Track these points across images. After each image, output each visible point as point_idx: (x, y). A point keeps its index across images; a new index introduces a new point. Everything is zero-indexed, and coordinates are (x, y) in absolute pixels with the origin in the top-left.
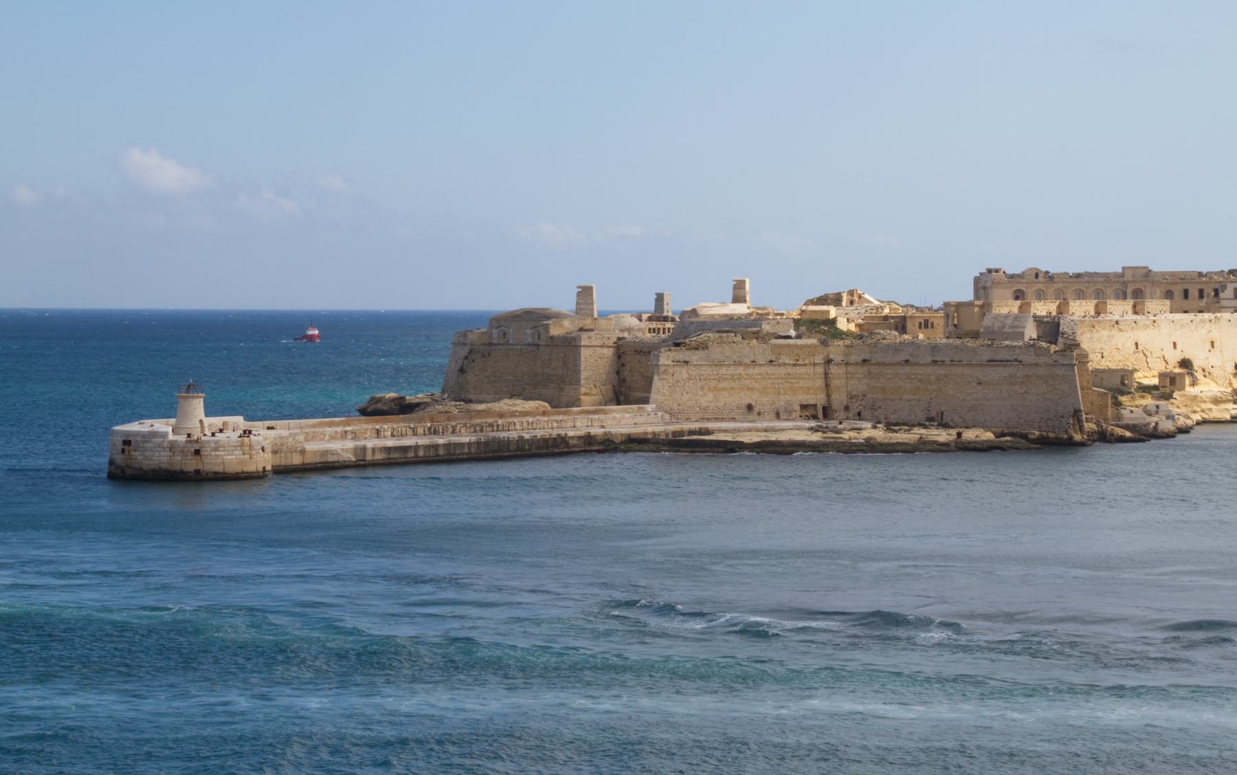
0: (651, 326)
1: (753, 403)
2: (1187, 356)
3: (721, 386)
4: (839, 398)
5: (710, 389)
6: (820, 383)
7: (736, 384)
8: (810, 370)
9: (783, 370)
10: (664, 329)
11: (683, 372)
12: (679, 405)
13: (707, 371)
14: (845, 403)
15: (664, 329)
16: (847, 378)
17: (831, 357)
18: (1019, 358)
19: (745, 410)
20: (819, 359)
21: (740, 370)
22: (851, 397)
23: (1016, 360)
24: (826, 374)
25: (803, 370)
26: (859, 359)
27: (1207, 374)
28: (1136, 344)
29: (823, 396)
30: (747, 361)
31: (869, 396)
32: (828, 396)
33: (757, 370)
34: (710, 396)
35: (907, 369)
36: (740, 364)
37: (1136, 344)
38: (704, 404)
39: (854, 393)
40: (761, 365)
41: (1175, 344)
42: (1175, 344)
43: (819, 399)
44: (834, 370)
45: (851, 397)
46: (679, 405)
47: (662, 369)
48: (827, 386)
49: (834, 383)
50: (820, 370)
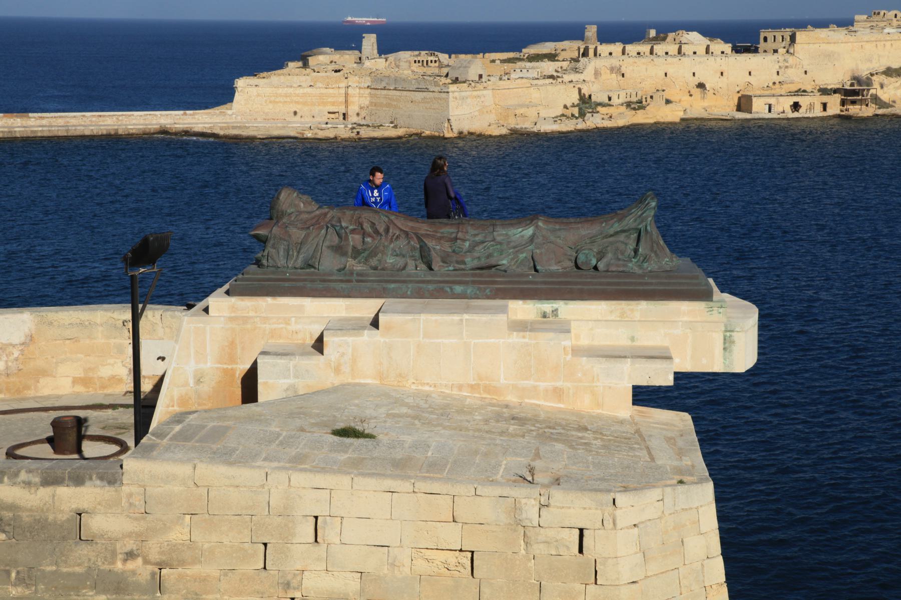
0: (416, 59)
1: (298, 111)
2: (702, 80)
3: (277, 100)
4: (353, 109)
5: (271, 102)
6: (342, 99)
7: (288, 99)
8: (336, 91)
9: (318, 91)
10: (427, 61)
11: (254, 91)
12: (250, 111)
13: (268, 90)
14: (357, 112)
15: (427, 61)
16: (359, 97)
17: (350, 84)
18: (428, 87)
19: (293, 115)
20: (343, 85)
21: (290, 90)
22: (361, 108)
23: (426, 88)
24: (347, 95)
25: (331, 91)
26: (366, 86)
27: (716, 92)
28: (666, 74)
29: (344, 107)
30: (295, 85)
31: (370, 108)
32: (347, 107)
33: (300, 91)
34: (271, 106)
35: (385, 92)
36: (291, 87)
37: (666, 74)
38: (266, 111)
39: (362, 106)
40: (304, 88)
41: (694, 74)
42: (694, 74)
43: (342, 109)
44: (350, 91)
45: (361, 108)
46: (250, 111)
47: (239, 89)
48: (346, 101)
49: (350, 99)
50: (343, 91)
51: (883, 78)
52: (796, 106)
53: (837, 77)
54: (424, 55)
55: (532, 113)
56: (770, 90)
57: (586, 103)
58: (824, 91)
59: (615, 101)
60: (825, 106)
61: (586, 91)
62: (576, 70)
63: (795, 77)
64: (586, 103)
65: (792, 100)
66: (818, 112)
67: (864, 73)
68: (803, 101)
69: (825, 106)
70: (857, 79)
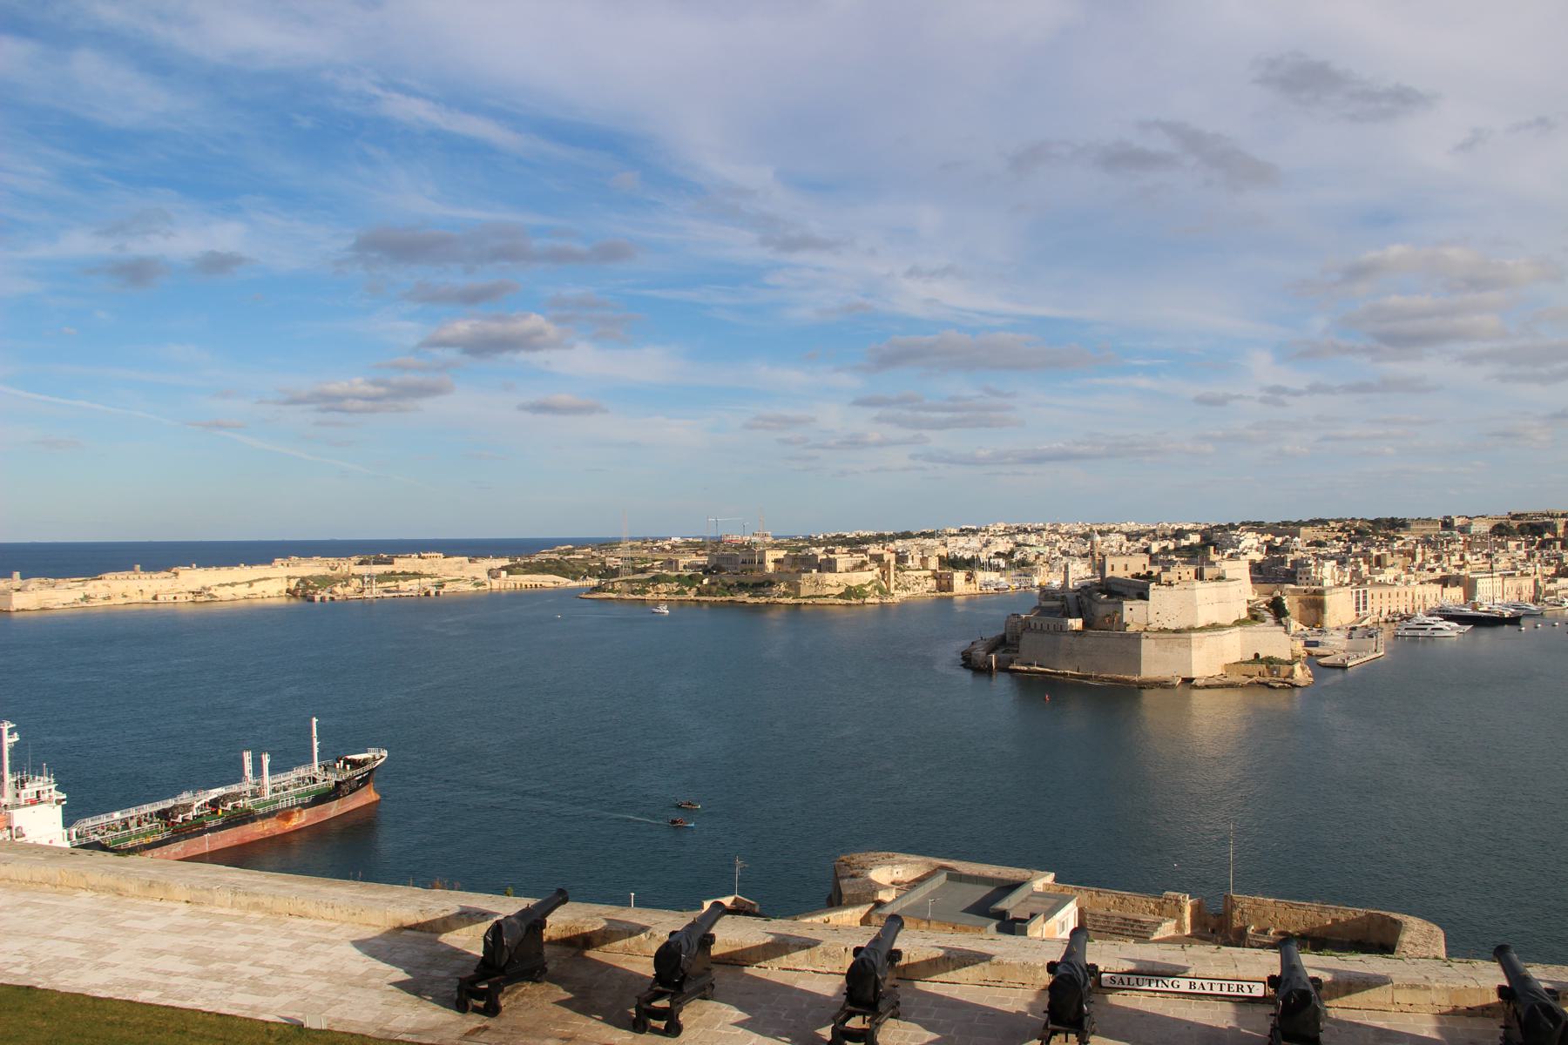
51: (216, 587)
52: (175, 598)
53: (196, 587)
54: (43, 580)
55: (54, 602)
56: (168, 593)
57: (86, 598)
58: (189, 592)
59: (99, 597)
60: (187, 598)
61: (87, 593)
62: (83, 586)
63: (179, 588)
64: (86, 598)
65: (173, 596)
66: (184, 600)
67: (208, 586)
68: (178, 596)
69: (187, 598)
70: (204, 588)
